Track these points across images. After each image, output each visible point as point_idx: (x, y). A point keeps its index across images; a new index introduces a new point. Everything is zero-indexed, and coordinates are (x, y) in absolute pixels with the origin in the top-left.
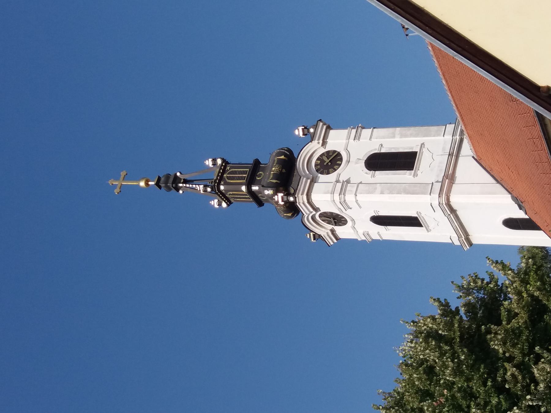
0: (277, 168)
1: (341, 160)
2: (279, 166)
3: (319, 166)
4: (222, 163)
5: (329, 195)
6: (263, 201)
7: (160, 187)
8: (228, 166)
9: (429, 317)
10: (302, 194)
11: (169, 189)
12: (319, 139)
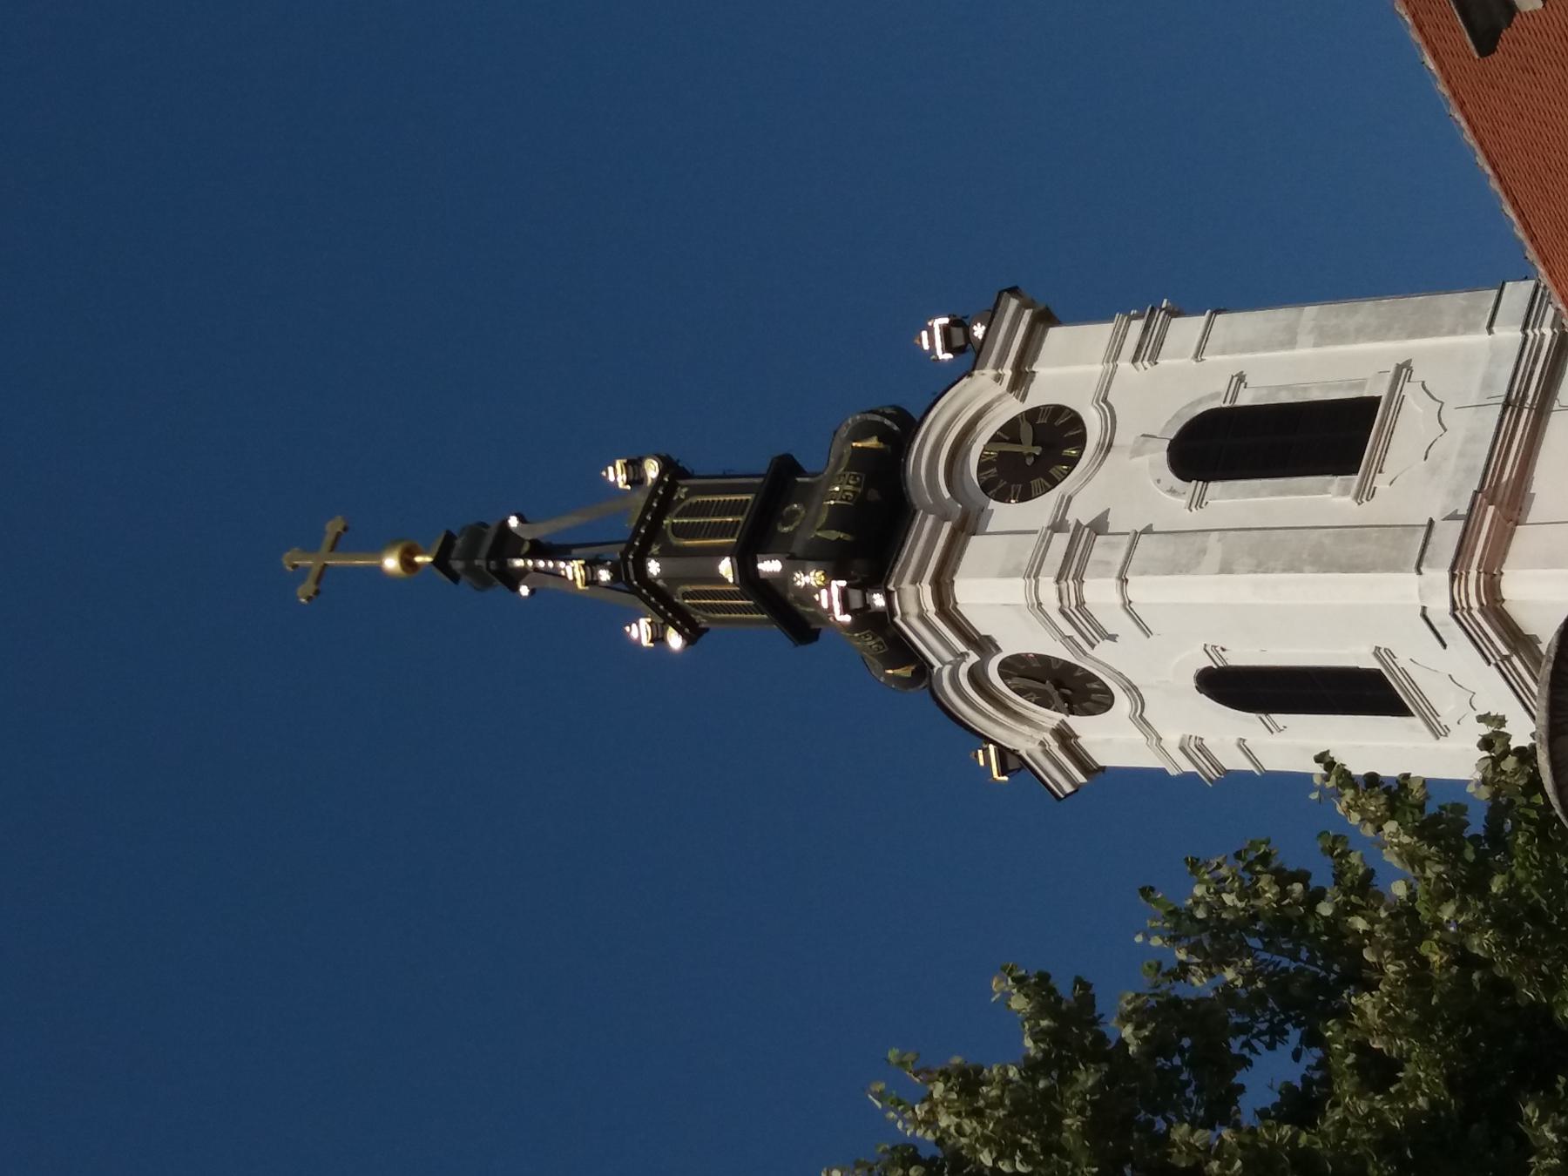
0: (848, 484)
1: (1080, 441)
2: (855, 476)
3: (994, 470)
5: (1020, 582)
6: (808, 618)
7: (454, 578)
8: (683, 487)
9: (946, 1076)
10: (916, 580)
11: (482, 580)
12: (999, 364)
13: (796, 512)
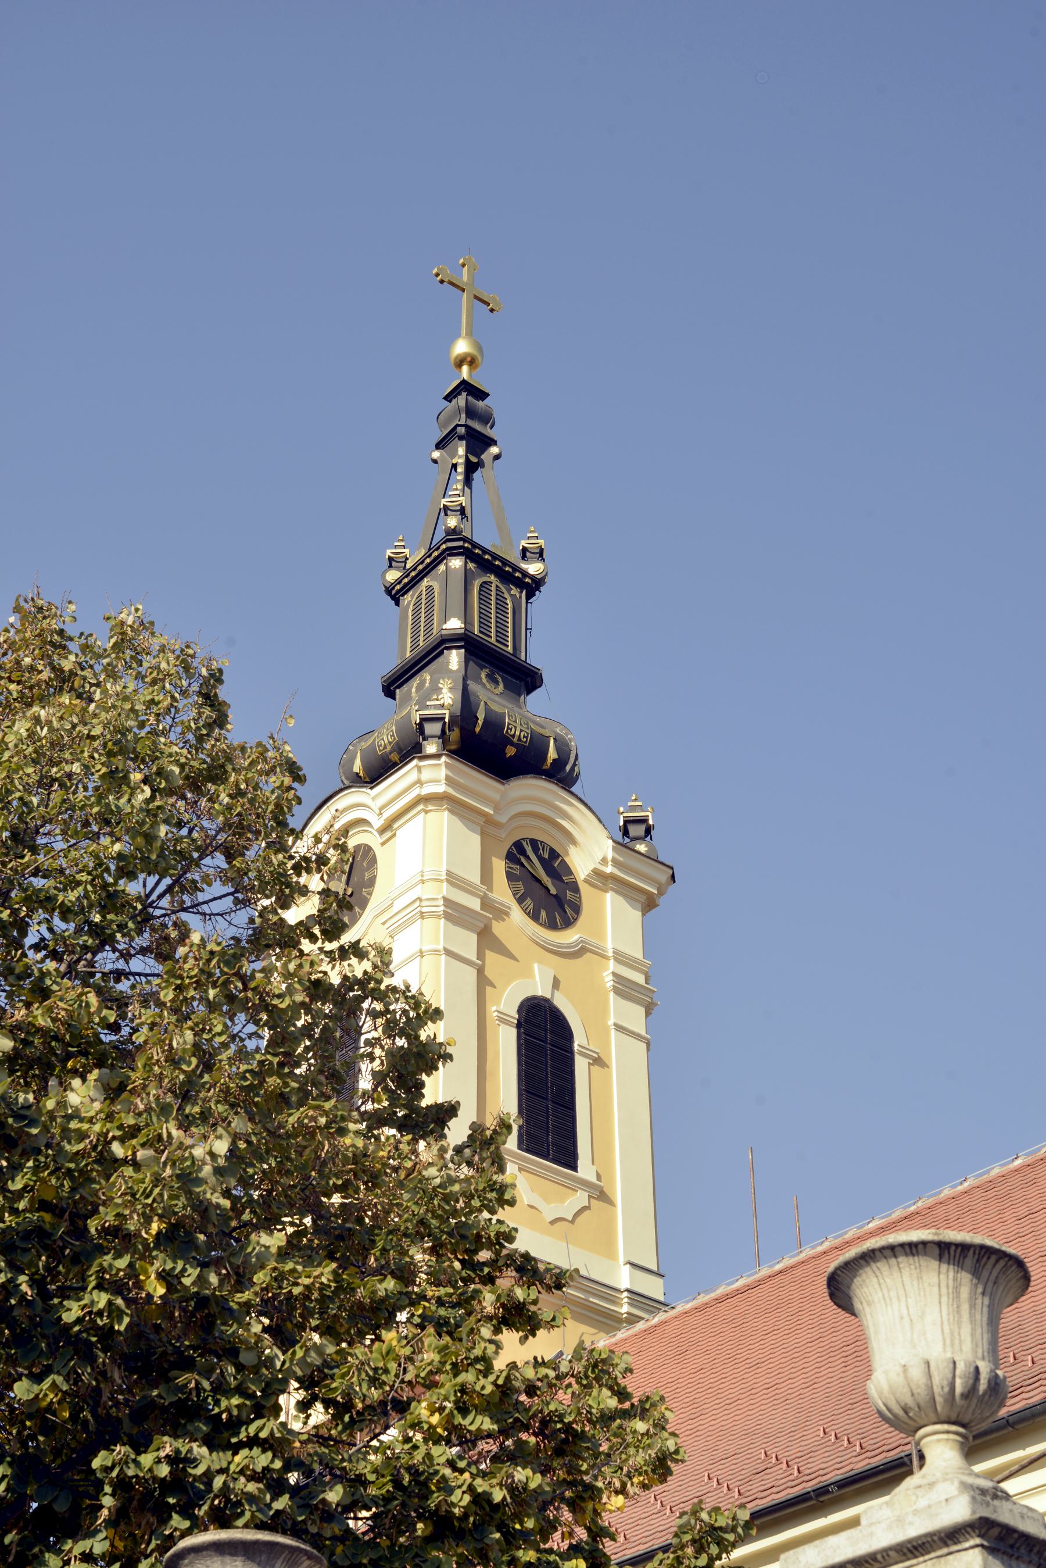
0: (521, 731)
1: (552, 926)
4: (532, 577)
6: (405, 687)
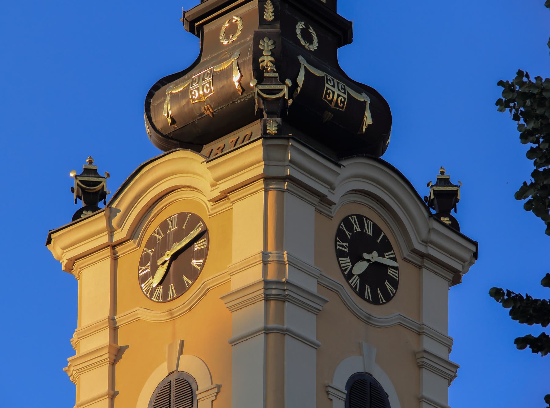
0: (339, 96)
3: (359, 230)
13: (311, 42)
